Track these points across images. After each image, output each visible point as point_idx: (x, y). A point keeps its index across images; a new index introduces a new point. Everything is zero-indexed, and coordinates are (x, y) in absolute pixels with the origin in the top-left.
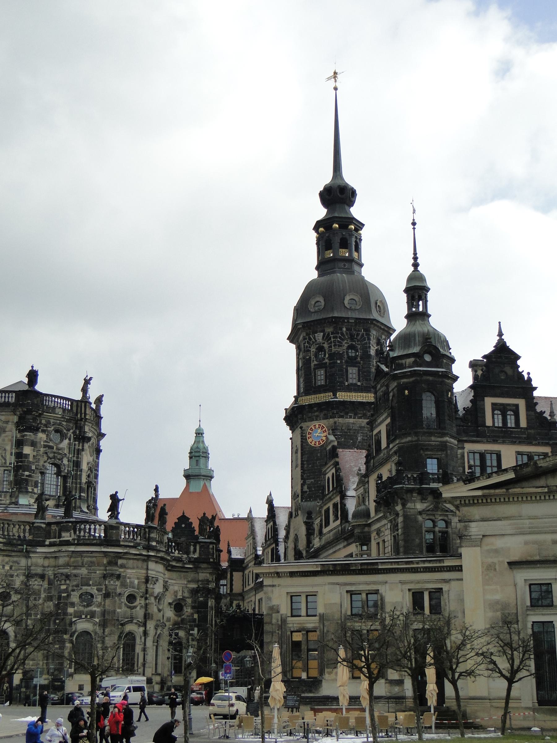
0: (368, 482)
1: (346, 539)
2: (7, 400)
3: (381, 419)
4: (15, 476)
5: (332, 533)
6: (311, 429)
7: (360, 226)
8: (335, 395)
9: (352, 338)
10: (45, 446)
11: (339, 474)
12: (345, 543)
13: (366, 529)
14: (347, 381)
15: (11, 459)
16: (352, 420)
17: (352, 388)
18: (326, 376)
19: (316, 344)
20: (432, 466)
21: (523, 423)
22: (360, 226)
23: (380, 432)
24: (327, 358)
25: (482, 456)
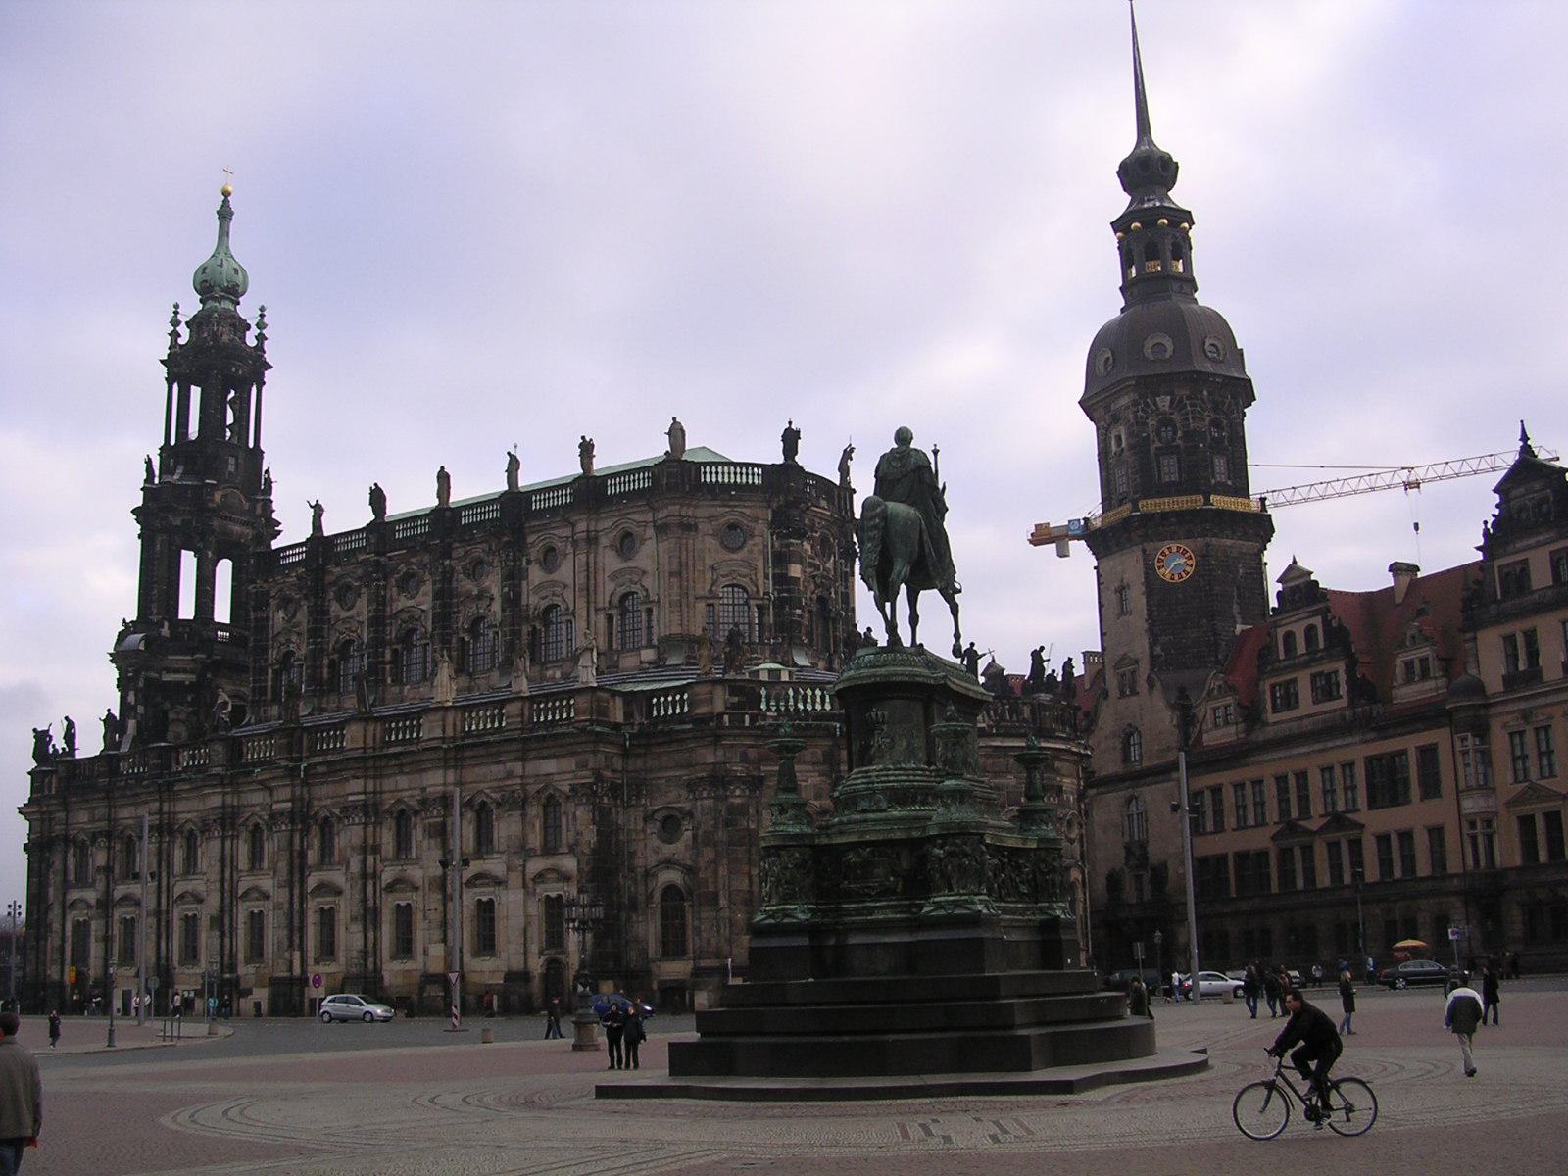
0: (1475, 638)
1: (1373, 729)
2: (714, 480)
3: (1532, 541)
4: (776, 615)
5: (1305, 722)
6: (1163, 553)
8: (1207, 501)
9: (1216, 408)
10: (812, 565)
11: (1340, 627)
12: (1372, 735)
13: (1482, 712)
14: (1214, 477)
15: (766, 586)
16: (1229, 542)
18: (1180, 467)
19: (1158, 415)
22: (1191, 223)
23: (1526, 560)
24: (1180, 438)
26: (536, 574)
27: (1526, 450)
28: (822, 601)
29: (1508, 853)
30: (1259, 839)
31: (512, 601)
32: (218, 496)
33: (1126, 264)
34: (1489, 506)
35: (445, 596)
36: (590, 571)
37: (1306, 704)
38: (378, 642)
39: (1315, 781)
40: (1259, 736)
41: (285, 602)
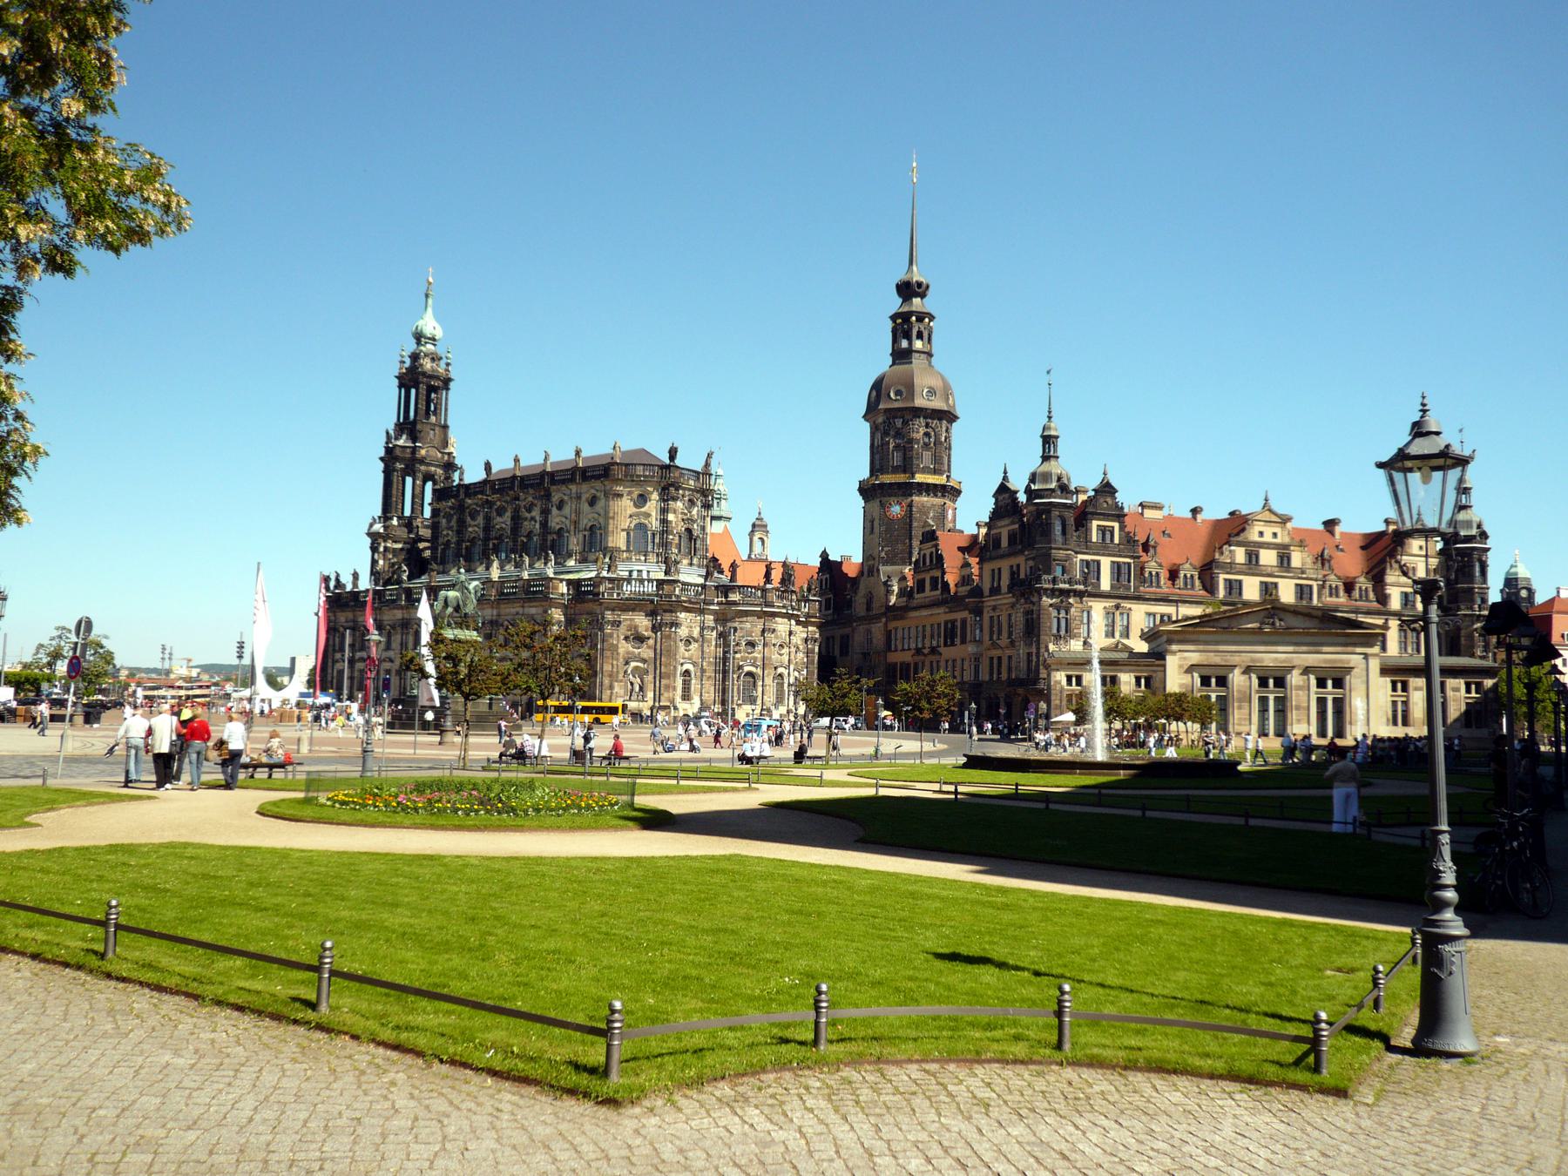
7: (932, 318)
9: (927, 426)
17: (926, 470)
20: (1059, 571)
21: (1116, 540)
25: (1088, 562)
26: (554, 511)
27: (1005, 478)
28: (689, 531)
29: (984, 676)
30: (907, 657)
31: (544, 524)
32: (423, 452)
33: (895, 340)
34: (990, 504)
35: (516, 519)
36: (578, 512)
37: (928, 592)
38: (487, 539)
39: (928, 629)
40: (914, 603)
41: (449, 517)
